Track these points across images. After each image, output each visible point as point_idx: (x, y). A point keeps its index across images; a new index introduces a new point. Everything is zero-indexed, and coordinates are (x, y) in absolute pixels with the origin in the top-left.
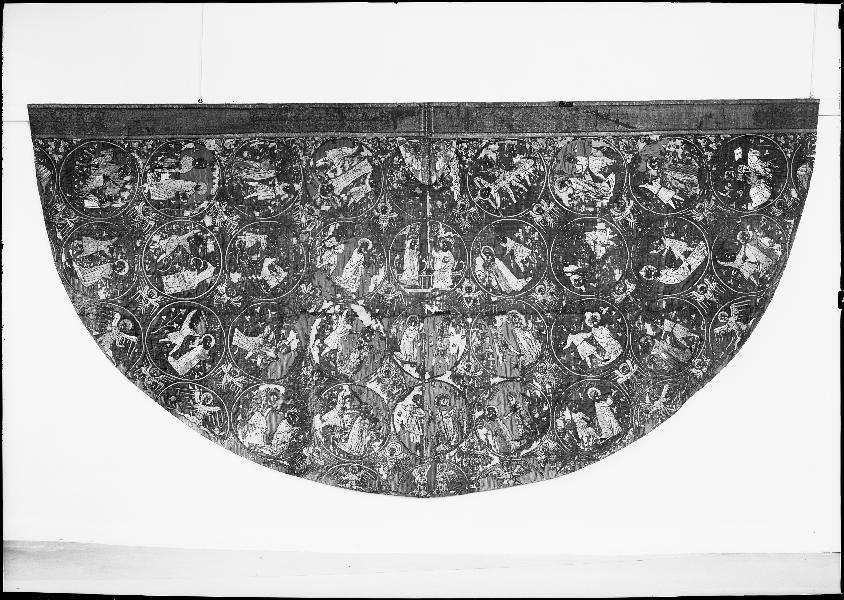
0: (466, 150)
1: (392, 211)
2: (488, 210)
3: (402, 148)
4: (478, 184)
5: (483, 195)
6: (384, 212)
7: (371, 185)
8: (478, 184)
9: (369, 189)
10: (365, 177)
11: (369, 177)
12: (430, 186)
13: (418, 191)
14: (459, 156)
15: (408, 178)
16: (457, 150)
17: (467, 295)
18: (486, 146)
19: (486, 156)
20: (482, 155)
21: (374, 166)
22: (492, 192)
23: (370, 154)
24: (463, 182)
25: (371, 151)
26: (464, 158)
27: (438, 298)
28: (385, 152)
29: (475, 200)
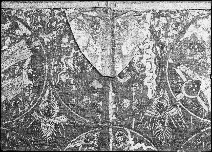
0: (166, 26)
1: (60, 114)
2: (197, 113)
3: (73, 24)
5: (188, 90)
6: (49, 115)
7: (30, 77)
9: (28, 82)
10: (21, 64)
11: (26, 65)
12: (112, 78)
13: (97, 85)
14: (155, 36)
15: (82, 67)
16: (151, 26)
18: (193, 21)
19: (194, 36)
20: (188, 34)
21: (34, 50)
22: (202, 87)
23: (28, 32)
24: (161, 75)
25: (29, 28)
26: (163, 39)
28: (51, 29)
29: (180, 97)
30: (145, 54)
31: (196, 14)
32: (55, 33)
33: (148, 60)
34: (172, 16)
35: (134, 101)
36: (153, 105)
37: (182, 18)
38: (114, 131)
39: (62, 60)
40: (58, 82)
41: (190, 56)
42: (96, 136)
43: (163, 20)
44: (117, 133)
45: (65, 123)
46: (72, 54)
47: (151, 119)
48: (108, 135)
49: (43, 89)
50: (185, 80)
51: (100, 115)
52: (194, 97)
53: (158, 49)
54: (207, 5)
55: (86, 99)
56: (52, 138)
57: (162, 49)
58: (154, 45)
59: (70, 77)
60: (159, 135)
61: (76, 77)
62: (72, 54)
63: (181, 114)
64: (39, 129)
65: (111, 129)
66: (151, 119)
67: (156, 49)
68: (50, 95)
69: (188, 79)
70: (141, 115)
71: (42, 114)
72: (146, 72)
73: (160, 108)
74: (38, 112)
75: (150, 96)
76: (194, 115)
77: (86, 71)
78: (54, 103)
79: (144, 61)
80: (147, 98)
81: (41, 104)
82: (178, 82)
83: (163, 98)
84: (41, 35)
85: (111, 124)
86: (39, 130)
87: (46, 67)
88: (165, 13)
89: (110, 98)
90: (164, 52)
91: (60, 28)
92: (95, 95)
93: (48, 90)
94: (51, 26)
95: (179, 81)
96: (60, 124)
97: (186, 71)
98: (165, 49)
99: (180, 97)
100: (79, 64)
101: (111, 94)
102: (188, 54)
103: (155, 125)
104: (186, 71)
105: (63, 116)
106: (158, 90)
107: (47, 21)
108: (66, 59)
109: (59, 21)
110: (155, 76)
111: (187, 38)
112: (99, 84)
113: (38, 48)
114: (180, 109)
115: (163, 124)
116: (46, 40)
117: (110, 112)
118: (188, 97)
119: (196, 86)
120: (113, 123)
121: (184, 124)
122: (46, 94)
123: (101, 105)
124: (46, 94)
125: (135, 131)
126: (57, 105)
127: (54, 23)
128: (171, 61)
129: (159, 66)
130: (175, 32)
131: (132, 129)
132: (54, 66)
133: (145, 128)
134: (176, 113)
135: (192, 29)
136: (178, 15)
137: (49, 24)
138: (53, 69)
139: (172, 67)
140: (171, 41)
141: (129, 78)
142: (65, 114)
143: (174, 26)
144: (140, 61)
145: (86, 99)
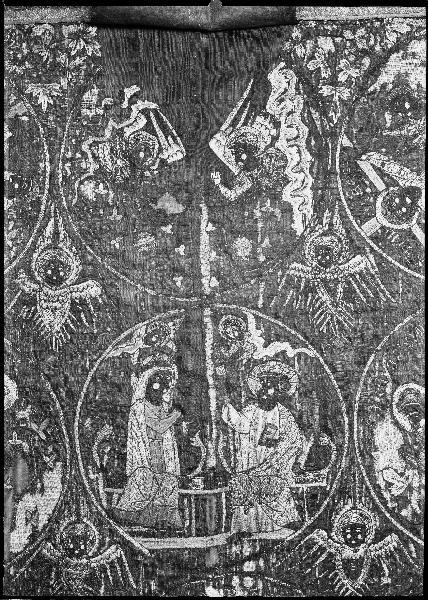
0: (332, 59)
1: (83, 277)
4: (373, 176)
6: (55, 281)
8: (373, 176)
17: (348, 552)
19: (401, 80)
20: (386, 77)
24: (323, 174)
27: (249, 566)
28: (54, 71)
29: (368, 228)
30: (283, 126)
31: (405, 29)
32: (64, 82)
33: (292, 143)
34: (348, 34)
35: (262, 242)
36: (308, 250)
37: (372, 39)
38: (215, 318)
39: (85, 147)
40: (74, 201)
41: (391, 129)
42: (172, 328)
43: (327, 45)
44: (223, 319)
45: (95, 298)
46: (108, 134)
47: (303, 285)
48: (201, 323)
49: (41, 216)
50: (380, 185)
51: (181, 278)
52: (405, 226)
53: (316, 115)
54: (421, 11)
55: (145, 241)
56: (66, 337)
57: (324, 113)
58: (306, 103)
59: (106, 188)
60: (324, 319)
61: (117, 188)
62: (108, 134)
63: (373, 268)
64: (34, 314)
65: (207, 312)
66: (303, 285)
67: (309, 113)
68: (56, 233)
69: (388, 186)
70: (280, 273)
71: (39, 279)
72: (288, 171)
73: (324, 257)
74: (29, 272)
75: (298, 227)
76: (406, 270)
77: (142, 175)
78: (67, 251)
79: (281, 144)
80: (293, 233)
81: (35, 255)
82: (365, 193)
83: (330, 231)
84: (31, 88)
85: (207, 300)
86: (33, 317)
87: (46, 166)
88: (329, 27)
89: (205, 238)
90: (330, 120)
91: (77, 68)
92: (168, 229)
93: (52, 220)
94: (56, 65)
95: (368, 190)
96: (83, 302)
97: (383, 164)
98: (331, 114)
99: (368, 228)
100: (126, 155)
101: (206, 227)
102: (388, 125)
103: (313, 297)
104: (383, 164)
105: (90, 282)
106: (318, 208)
107: (45, 54)
108: (96, 143)
109: (73, 53)
110: (310, 181)
111: (384, 86)
112: (174, 204)
113: (25, 118)
114: (371, 257)
115: (332, 292)
116: (44, 101)
117: (205, 269)
118: (389, 228)
119: (408, 201)
120: (211, 297)
121: (382, 291)
122: (50, 228)
123: (182, 253)
124: (50, 228)
125: (265, 313)
126: (75, 254)
127: (62, 58)
128: (346, 142)
129: (320, 154)
130: (354, 73)
131: (257, 308)
132: (65, 160)
133: (290, 305)
134: (362, 266)
135: (395, 65)
136: (361, 32)
137: (51, 60)
138: (64, 169)
139: (351, 159)
140: (346, 94)
141: (248, 185)
142: (94, 277)
143: (352, 58)
144: (272, 145)
145: (145, 241)
